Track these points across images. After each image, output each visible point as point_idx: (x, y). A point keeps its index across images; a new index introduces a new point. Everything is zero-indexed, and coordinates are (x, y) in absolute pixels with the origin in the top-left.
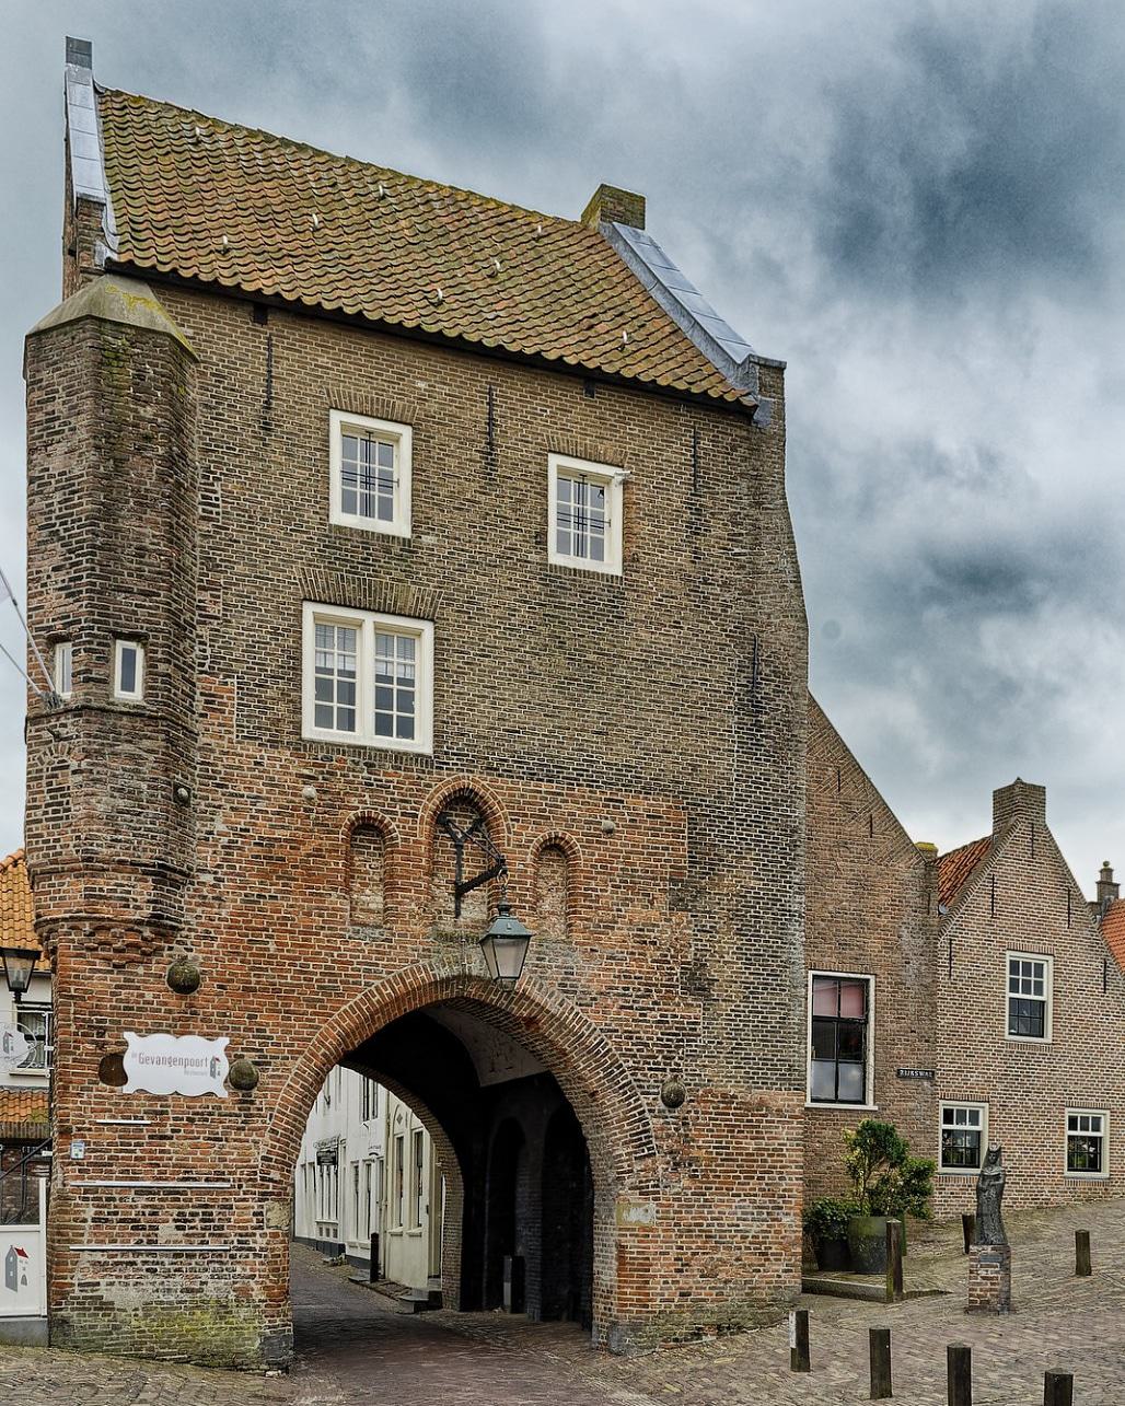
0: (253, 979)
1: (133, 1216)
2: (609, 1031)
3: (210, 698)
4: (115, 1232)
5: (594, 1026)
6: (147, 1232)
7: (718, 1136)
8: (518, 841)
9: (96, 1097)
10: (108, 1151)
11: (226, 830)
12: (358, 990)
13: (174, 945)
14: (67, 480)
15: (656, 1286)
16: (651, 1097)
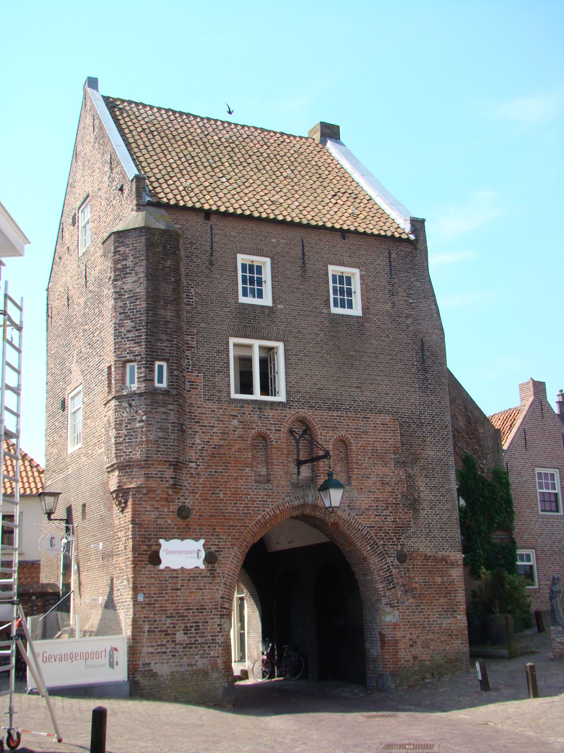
0: (214, 511)
1: (165, 629)
2: (371, 527)
5: (364, 525)
7: (425, 576)
9: (148, 571)
10: (153, 597)
11: (200, 442)
12: (260, 514)
13: (180, 497)
15: (402, 654)
16: (392, 558)
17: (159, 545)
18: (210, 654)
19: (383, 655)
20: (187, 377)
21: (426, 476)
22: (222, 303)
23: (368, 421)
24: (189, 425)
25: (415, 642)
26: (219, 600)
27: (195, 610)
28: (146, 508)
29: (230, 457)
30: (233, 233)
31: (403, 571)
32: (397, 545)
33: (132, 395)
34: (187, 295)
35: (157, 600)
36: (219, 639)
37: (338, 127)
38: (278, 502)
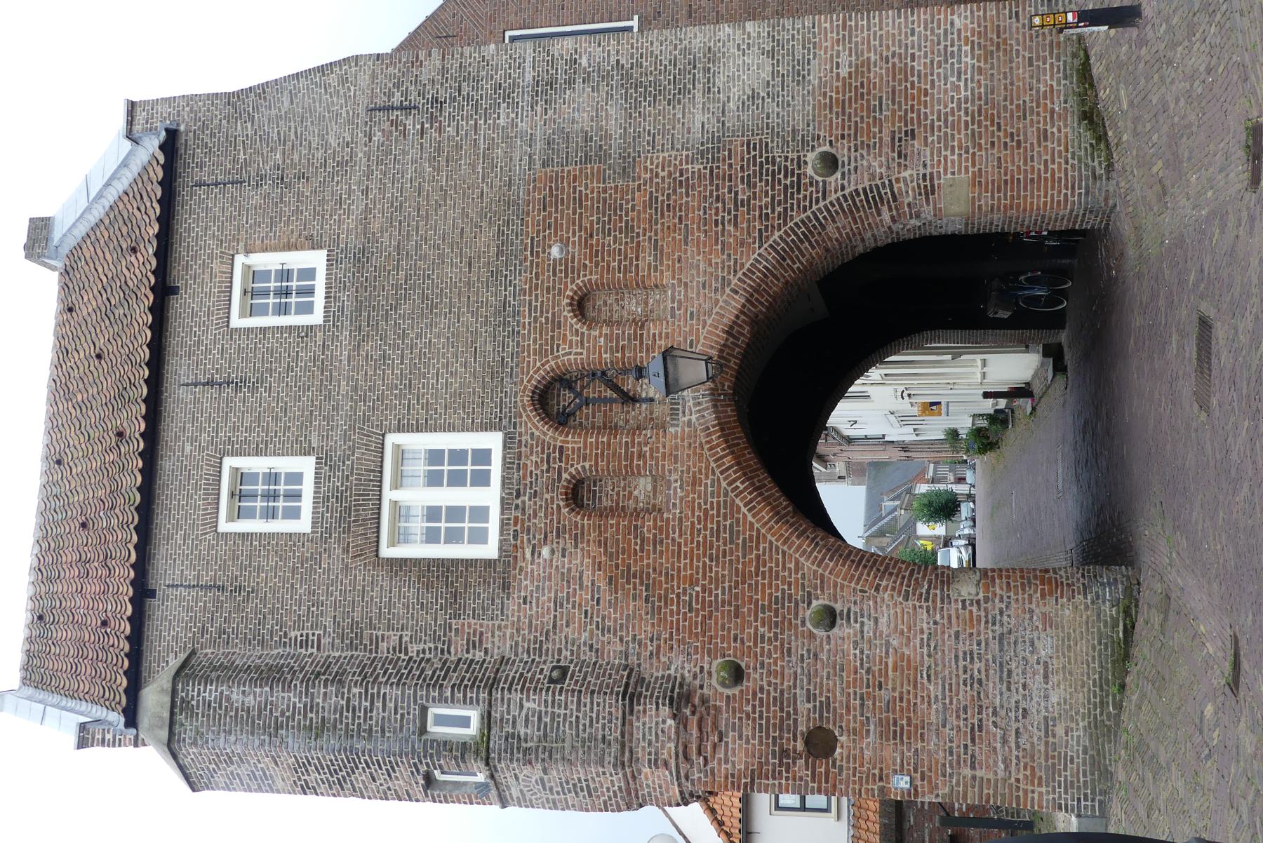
0: (726, 608)
3: (471, 645)
6: (984, 716)
9: (848, 762)
14: (300, 767)
26: (910, 603)
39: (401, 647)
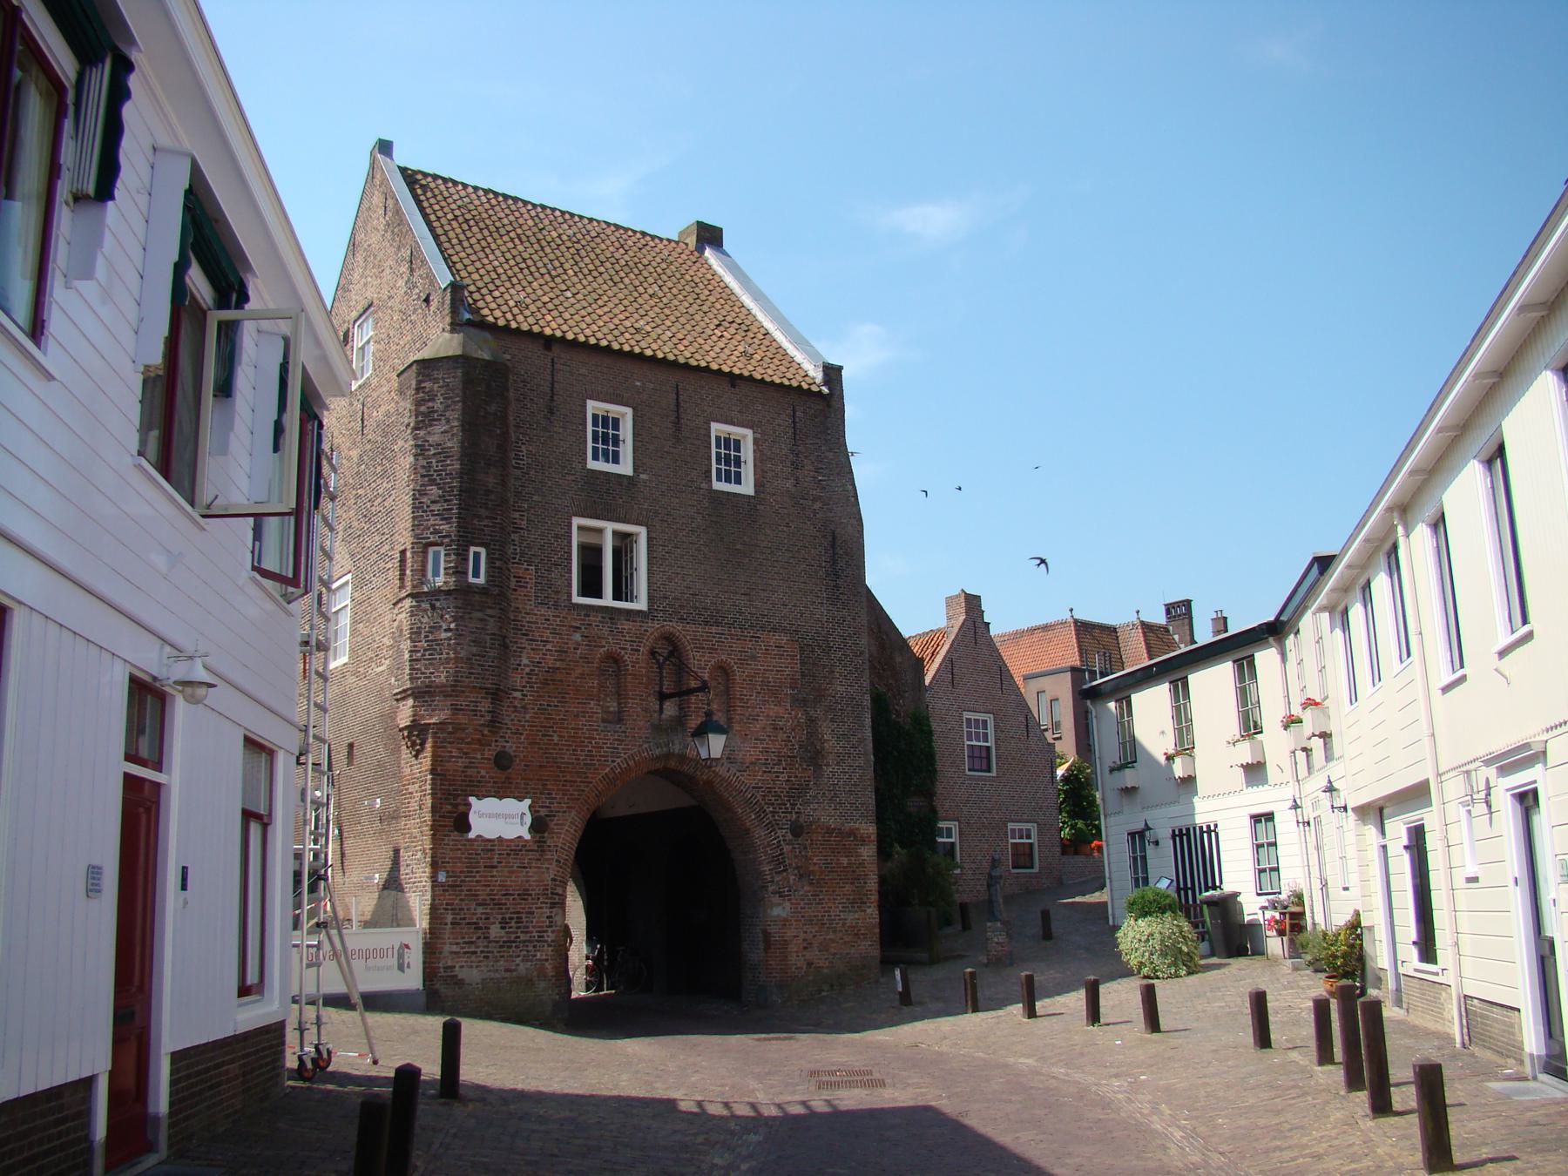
0: (545, 760)
1: (475, 920)
2: (757, 788)
4: (464, 931)
8: (701, 663)
9: (453, 840)
10: (460, 877)
12: (608, 766)
15: (793, 959)
16: (784, 831)
17: (469, 805)
18: (535, 956)
19: (767, 961)
20: (512, 571)
21: (832, 720)
22: (564, 468)
23: (758, 642)
24: (514, 638)
25: (811, 944)
26: (550, 883)
27: (516, 896)
28: (451, 752)
29: (569, 686)
30: (583, 371)
31: (799, 848)
32: (791, 813)
33: (436, 593)
34: (516, 455)
35: (464, 881)
36: (548, 936)
37: (722, 229)
38: (632, 750)
39: (518, 529)
